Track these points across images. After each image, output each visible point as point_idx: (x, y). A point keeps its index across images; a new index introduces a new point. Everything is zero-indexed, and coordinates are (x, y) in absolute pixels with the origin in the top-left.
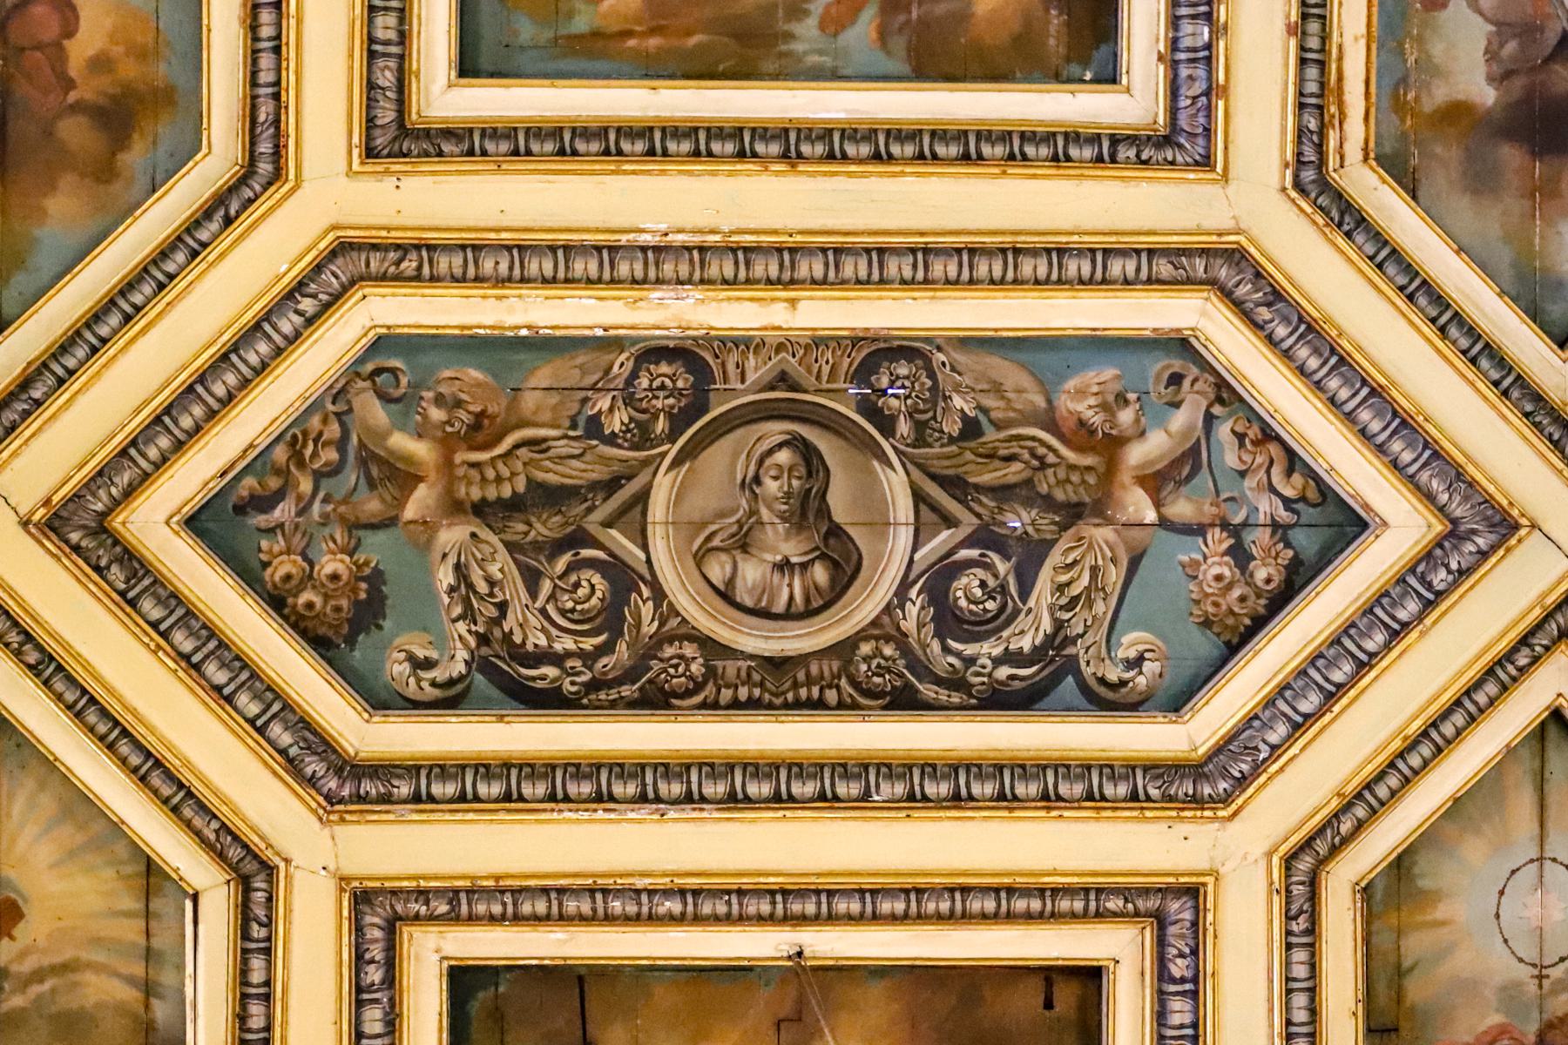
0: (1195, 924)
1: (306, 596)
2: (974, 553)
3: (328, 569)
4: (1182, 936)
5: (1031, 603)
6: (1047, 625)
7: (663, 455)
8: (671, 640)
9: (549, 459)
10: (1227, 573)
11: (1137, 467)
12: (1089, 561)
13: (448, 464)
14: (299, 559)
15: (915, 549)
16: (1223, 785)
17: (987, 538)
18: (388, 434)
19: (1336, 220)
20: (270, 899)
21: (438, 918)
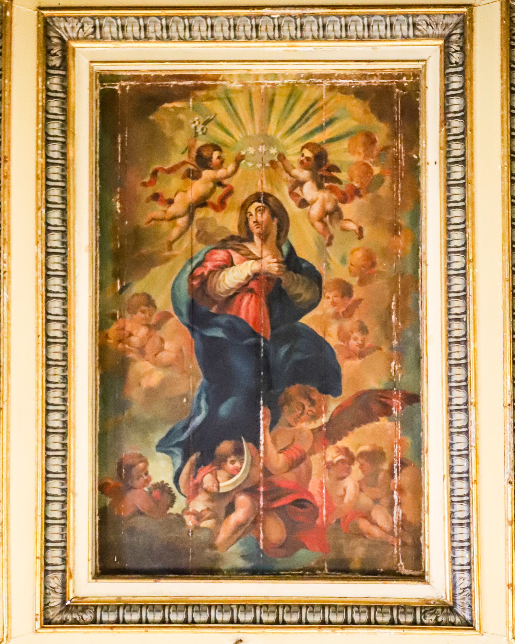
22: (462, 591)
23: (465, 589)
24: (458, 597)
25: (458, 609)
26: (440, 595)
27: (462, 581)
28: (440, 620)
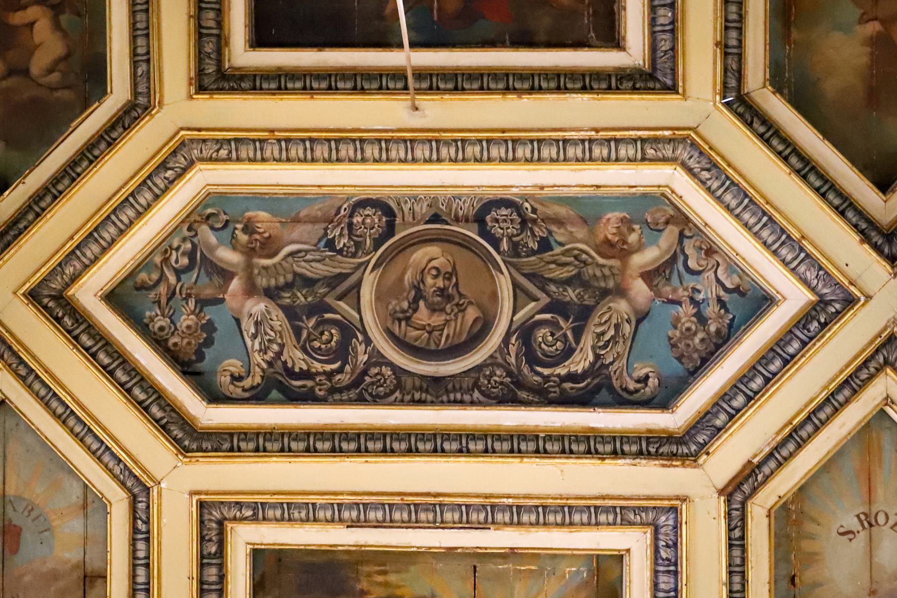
0: (675, 527)
1: (175, 340)
2: (548, 316)
3: (185, 325)
4: (667, 535)
5: (581, 345)
6: (591, 358)
7: (369, 261)
8: (376, 364)
9: (304, 261)
10: (693, 327)
11: (641, 267)
12: (614, 321)
13: (249, 266)
14: (169, 320)
15: (514, 313)
16: (693, 448)
17: (557, 307)
18: (217, 247)
19: (749, 121)
20: (148, 507)
21: (246, 519)
22: (663, 54)
23: (666, 51)
24: (659, 61)
25: (659, 75)
26: (637, 62)
27: (663, 42)
28: (638, 86)
